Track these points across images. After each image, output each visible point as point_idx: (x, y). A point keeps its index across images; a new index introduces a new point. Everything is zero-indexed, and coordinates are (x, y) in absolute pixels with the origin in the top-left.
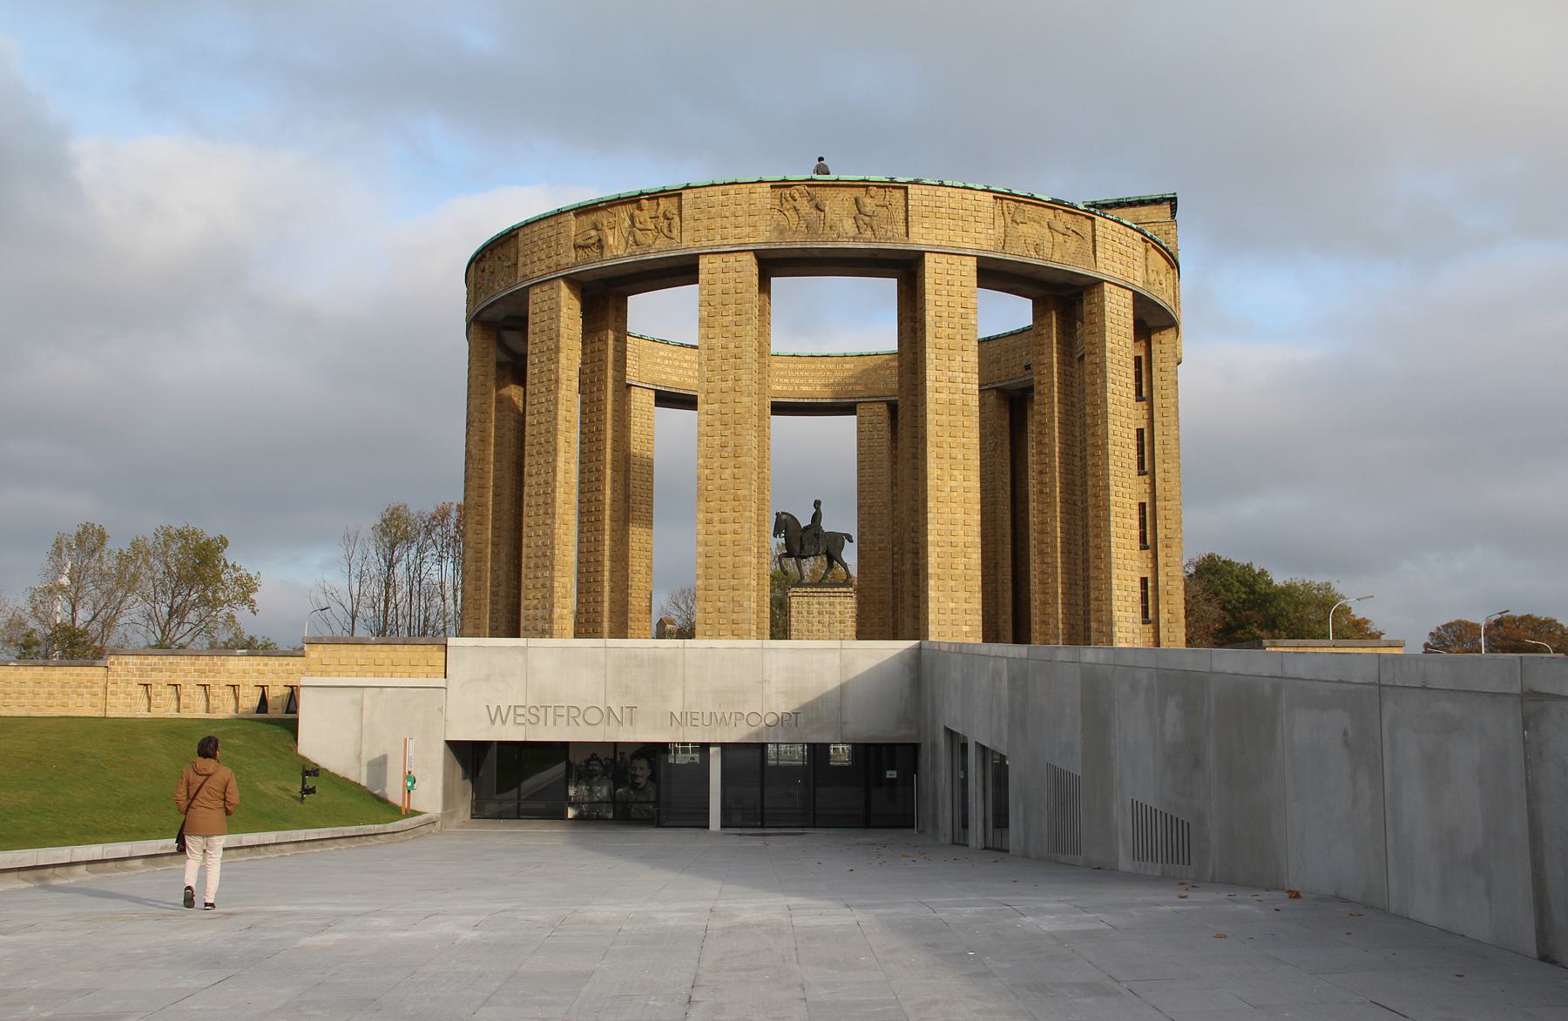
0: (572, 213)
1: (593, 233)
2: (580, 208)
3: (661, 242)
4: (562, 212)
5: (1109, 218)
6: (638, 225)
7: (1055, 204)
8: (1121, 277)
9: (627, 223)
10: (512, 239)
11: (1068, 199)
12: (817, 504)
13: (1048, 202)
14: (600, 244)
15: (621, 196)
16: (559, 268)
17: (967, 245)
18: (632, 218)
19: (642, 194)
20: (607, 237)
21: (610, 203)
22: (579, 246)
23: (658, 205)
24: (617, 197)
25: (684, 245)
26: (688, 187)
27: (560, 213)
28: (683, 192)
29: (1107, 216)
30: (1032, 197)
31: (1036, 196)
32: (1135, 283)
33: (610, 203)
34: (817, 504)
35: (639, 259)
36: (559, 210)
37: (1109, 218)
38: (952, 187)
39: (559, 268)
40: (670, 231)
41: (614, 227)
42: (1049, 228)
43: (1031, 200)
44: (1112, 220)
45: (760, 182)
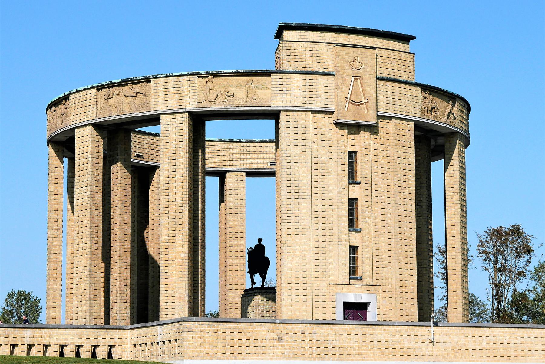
5: (160, 77)
7: (124, 83)
8: (173, 108)
11: (129, 76)
12: (260, 240)
13: (120, 82)
17: (86, 119)
29: (159, 76)
30: (111, 83)
31: (113, 82)
32: (187, 107)
34: (260, 240)
37: (160, 77)
38: (85, 89)
42: (125, 96)
43: (111, 85)
44: (163, 77)
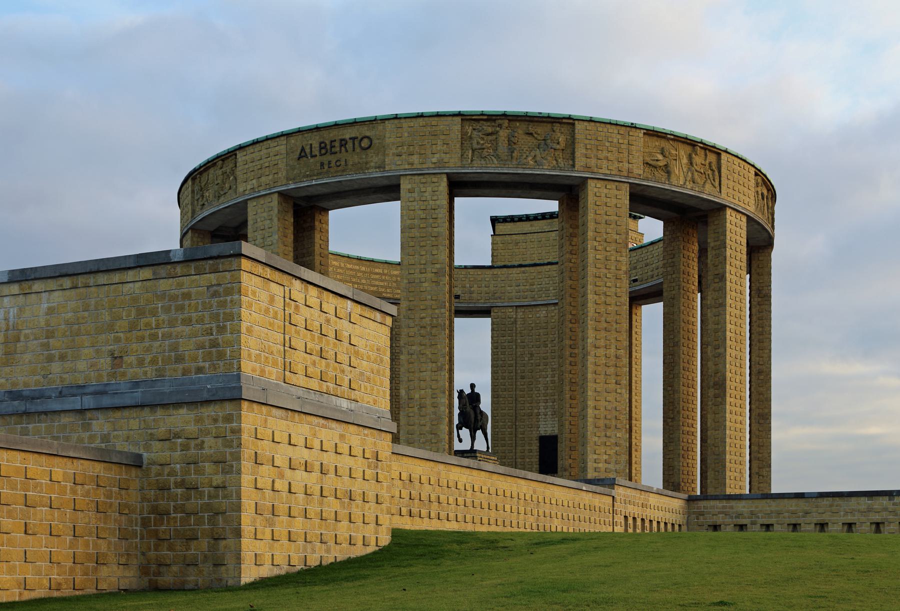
0: (642, 131)
1: (660, 157)
2: (653, 131)
3: (708, 186)
4: (635, 127)
6: (695, 166)
9: (685, 161)
10: (558, 125)
12: (473, 386)
14: (667, 170)
15: (689, 138)
16: (630, 175)
18: (690, 158)
19: (701, 143)
20: (673, 165)
21: (676, 138)
22: (647, 163)
23: (706, 155)
24: (685, 136)
25: (724, 195)
26: (726, 151)
27: (633, 126)
28: (722, 153)
33: (676, 138)
34: (473, 386)
35: (697, 195)
36: (632, 124)
39: (630, 175)
40: (714, 180)
41: (676, 160)
45: (753, 166)
